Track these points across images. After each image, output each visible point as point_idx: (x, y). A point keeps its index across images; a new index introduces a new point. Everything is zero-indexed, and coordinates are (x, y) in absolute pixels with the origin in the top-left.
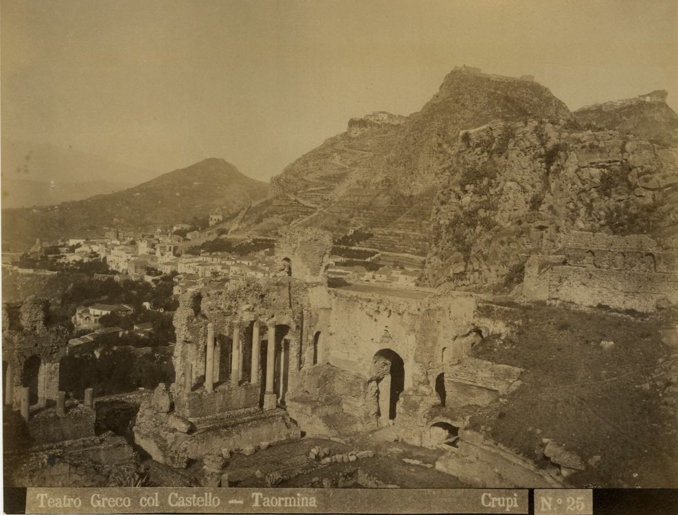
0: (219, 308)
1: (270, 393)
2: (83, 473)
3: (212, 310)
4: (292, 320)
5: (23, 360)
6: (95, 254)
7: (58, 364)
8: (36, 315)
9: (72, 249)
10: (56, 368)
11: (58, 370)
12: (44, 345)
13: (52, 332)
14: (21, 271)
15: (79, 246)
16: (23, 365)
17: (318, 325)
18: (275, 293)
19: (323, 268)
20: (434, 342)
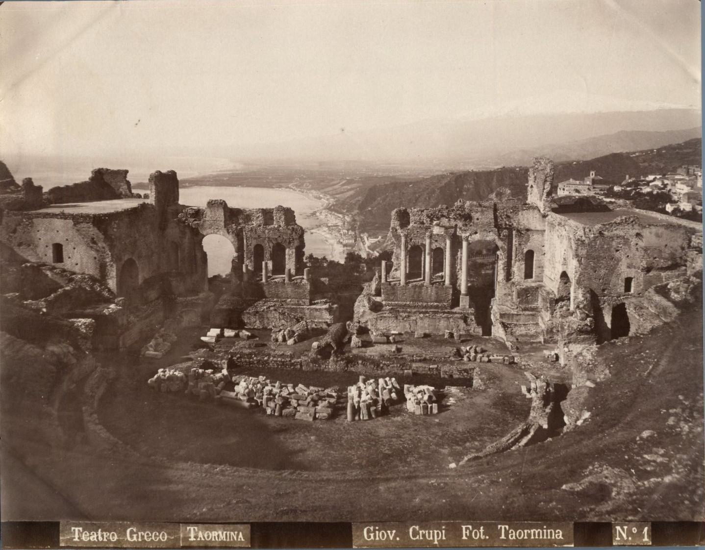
1: (463, 295)
4: (496, 237)
5: (271, 245)
6: (665, 186)
7: (294, 250)
8: (280, 218)
9: (648, 184)
10: (292, 252)
11: (294, 254)
13: (289, 229)
14: (605, 200)
15: (654, 180)
17: (529, 244)
18: (479, 214)
19: (545, 195)
20: (612, 270)
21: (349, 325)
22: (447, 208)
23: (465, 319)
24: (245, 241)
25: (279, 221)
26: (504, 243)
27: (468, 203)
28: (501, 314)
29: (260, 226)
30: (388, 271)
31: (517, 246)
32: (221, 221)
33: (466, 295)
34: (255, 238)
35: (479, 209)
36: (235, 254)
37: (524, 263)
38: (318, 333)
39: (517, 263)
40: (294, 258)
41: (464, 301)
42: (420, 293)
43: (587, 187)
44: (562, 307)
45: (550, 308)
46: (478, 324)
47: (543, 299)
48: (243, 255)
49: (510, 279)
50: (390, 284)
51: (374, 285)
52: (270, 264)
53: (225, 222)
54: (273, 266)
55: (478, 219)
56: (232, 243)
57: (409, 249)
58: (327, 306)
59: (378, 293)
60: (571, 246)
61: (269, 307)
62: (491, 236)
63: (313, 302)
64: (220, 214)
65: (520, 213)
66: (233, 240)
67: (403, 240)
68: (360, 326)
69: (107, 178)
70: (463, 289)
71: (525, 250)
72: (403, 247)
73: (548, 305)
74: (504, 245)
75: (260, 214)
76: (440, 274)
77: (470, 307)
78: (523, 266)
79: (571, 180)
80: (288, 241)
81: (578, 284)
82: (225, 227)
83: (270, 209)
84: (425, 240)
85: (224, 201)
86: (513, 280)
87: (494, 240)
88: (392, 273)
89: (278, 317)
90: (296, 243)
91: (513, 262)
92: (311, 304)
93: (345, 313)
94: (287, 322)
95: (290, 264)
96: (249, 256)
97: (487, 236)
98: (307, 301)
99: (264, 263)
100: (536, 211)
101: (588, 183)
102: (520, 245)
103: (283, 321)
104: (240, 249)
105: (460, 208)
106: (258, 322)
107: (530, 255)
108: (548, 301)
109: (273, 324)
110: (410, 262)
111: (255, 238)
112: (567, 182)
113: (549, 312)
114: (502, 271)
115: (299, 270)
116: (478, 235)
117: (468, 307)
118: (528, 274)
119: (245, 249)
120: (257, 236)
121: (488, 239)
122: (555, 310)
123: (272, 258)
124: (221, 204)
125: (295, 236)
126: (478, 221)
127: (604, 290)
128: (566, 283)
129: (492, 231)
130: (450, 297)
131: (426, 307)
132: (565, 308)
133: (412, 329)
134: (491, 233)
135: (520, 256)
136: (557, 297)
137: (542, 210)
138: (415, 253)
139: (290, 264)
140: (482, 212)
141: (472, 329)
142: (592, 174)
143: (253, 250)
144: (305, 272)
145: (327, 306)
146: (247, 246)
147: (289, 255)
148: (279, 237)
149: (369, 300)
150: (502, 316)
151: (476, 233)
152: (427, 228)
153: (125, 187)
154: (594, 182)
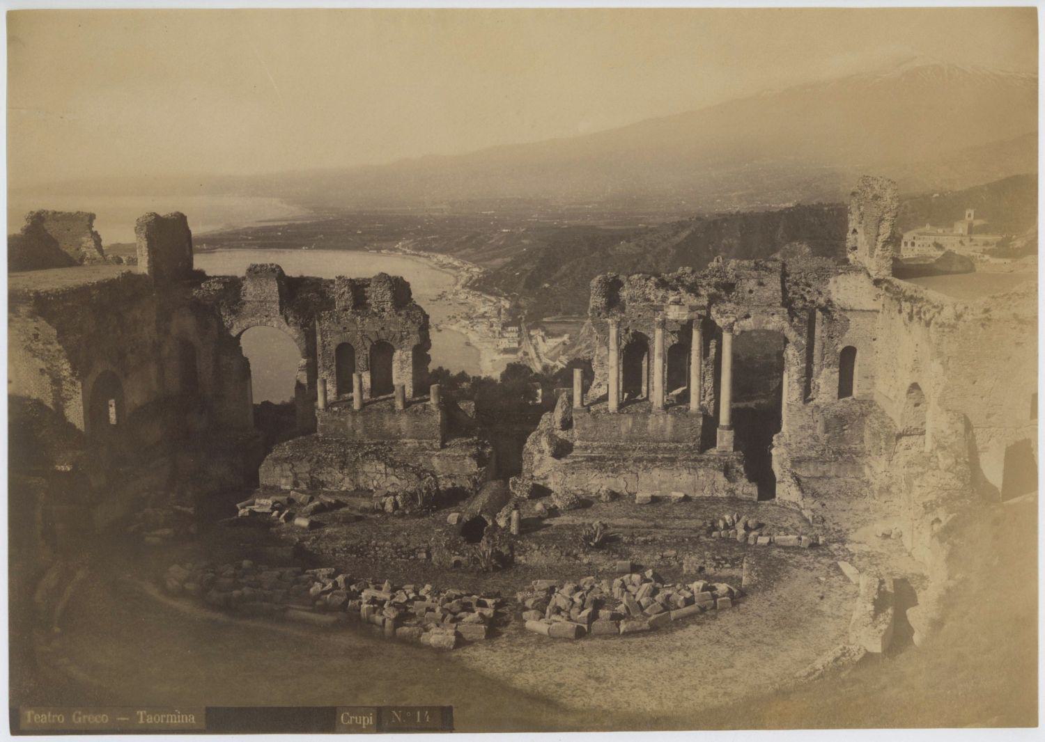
0: (648, 300)
1: (723, 428)
2: (403, 477)
3: (635, 301)
4: (786, 325)
5: (368, 344)
7: (411, 353)
8: (383, 295)
10: (408, 357)
11: (411, 360)
12: (392, 329)
16: (368, 349)
17: (847, 336)
21: (514, 484)
22: (693, 272)
23: (727, 470)
24: (319, 338)
25: (379, 297)
26: (800, 334)
27: (733, 263)
28: (792, 461)
29: (346, 310)
30: (585, 390)
31: (826, 339)
32: (274, 302)
33: (729, 428)
34: (338, 332)
35: (754, 273)
36: (303, 361)
37: (837, 370)
38: (455, 497)
39: (825, 371)
40: (411, 367)
41: (725, 439)
42: (646, 425)
43: (959, 239)
44: (908, 448)
45: (886, 449)
46: (751, 479)
47: (874, 434)
48: (315, 362)
49: (812, 399)
50: (589, 410)
51: (558, 414)
52: (367, 378)
53: (281, 303)
54: (372, 381)
55: (751, 292)
56: (296, 341)
57: (622, 346)
58: (474, 450)
59: (567, 424)
60: (929, 337)
61: (367, 454)
62: (776, 322)
63: (448, 444)
64: (272, 288)
65: (832, 280)
66: (297, 336)
67: (613, 332)
68: (534, 485)
69: (51, 228)
70: (724, 418)
71: (840, 347)
72: (613, 345)
73: (883, 444)
74: (799, 338)
75: (346, 289)
76: (679, 391)
77: (736, 449)
78: (836, 376)
79: (928, 227)
80: (398, 336)
81: (939, 405)
82: (281, 313)
83: (364, 280)
84: (654, 331)
85: (278, 266)
86: (816, 401)
87: (783, 329)
88: (590, 393)
89: (383, 471)
90: (415, 339)
91: (815, 369)
92: (443, 446)
93: (504, 463)
94: (401, 479)
95: (402, 375)
96: (328, 364)
97: (768, 322)
98: (437, 445)
99: (355, 377)
100: (862, 276)
101: (961, 231)
102: (831, 337)
103: (393, 478)
104: (310, 352)
105: (717, 271)
106: (347, 479)
107: (847, 358)
108: (883, 436)
109: (375, 483)
110: (624, 371)
111: (338, 332)
112: (921, 230)
113: (884, 458)
114: (797, 386)
115: (421, 388)
116: (750, 320)
117: (732, 449)
118: (845, 388)
119: (319, 351)
120: (341, 329)
121: (770, 327)
122: (895, 453)
123: (371, 368)
124: (273, 270)
125: (415, 328)
126: (751, 296)
127: (988, 416)
128: (917, 405)
129: (778, 312)
130: (699, 432)
131: (655, 451)
132: (914, 450)
133: (629, 490)
134: (776, 318)
135: (830, 358)
136: (900, 428)
137: (872, 273)
138: (634, 352)
139: (402, 375)
141: (741, 489)
142: (969, 216)
143: (334, 353)
144: (432, 391)
145: (474, 450)
146: (324, 346)
147: (402, 362)
148: (383, 329)
149: (552, 437)
150: (797, 462)
151: (747, 316)
152: (657, 309)
153: (92, 244)
154: (971, 230)
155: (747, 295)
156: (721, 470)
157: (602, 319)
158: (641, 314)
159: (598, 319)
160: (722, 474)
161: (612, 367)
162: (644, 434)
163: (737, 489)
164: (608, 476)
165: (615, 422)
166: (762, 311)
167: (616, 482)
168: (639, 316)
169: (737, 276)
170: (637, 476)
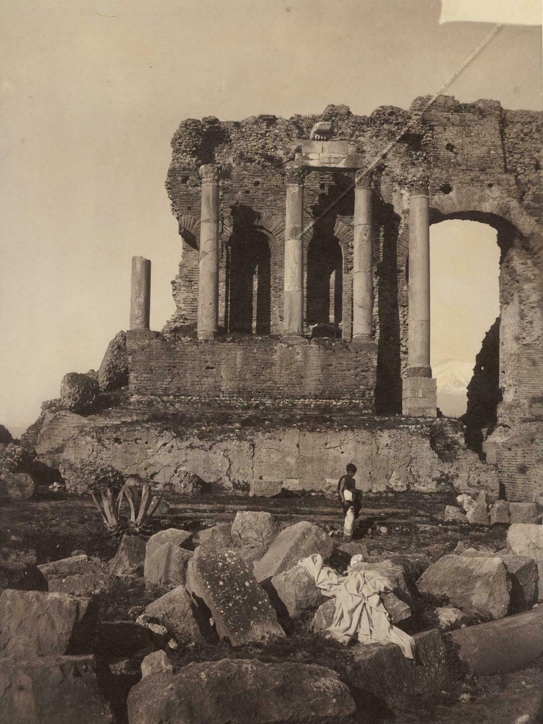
4: (514, 203)
55: (450, 147)
87: (508, 211)
97: (482, 199)
134: (496, 192)
140: (463, 124)
155: (444, 153)
156: (424, 436)
157: (190, 188)
158: (259, 179)
159: (182, 186)
160: (427, 444)
161: (205, 253)
162: (266, 381)
163: (457, 476)
164: (191, 447)
165: (208, 357)
166: (472, 180)
167: (208, 457)
168: (257, 183)
169: (424, 121)
170: (253, 446)
